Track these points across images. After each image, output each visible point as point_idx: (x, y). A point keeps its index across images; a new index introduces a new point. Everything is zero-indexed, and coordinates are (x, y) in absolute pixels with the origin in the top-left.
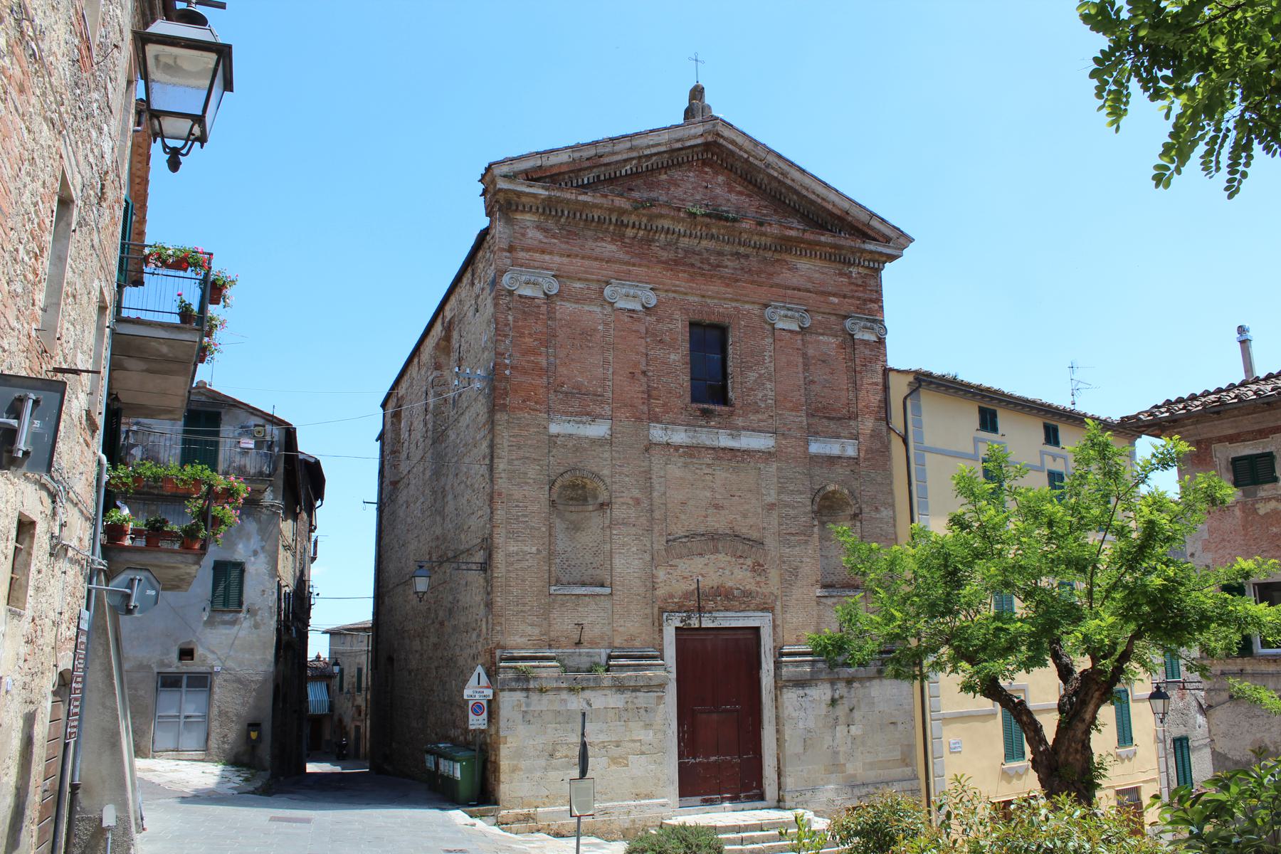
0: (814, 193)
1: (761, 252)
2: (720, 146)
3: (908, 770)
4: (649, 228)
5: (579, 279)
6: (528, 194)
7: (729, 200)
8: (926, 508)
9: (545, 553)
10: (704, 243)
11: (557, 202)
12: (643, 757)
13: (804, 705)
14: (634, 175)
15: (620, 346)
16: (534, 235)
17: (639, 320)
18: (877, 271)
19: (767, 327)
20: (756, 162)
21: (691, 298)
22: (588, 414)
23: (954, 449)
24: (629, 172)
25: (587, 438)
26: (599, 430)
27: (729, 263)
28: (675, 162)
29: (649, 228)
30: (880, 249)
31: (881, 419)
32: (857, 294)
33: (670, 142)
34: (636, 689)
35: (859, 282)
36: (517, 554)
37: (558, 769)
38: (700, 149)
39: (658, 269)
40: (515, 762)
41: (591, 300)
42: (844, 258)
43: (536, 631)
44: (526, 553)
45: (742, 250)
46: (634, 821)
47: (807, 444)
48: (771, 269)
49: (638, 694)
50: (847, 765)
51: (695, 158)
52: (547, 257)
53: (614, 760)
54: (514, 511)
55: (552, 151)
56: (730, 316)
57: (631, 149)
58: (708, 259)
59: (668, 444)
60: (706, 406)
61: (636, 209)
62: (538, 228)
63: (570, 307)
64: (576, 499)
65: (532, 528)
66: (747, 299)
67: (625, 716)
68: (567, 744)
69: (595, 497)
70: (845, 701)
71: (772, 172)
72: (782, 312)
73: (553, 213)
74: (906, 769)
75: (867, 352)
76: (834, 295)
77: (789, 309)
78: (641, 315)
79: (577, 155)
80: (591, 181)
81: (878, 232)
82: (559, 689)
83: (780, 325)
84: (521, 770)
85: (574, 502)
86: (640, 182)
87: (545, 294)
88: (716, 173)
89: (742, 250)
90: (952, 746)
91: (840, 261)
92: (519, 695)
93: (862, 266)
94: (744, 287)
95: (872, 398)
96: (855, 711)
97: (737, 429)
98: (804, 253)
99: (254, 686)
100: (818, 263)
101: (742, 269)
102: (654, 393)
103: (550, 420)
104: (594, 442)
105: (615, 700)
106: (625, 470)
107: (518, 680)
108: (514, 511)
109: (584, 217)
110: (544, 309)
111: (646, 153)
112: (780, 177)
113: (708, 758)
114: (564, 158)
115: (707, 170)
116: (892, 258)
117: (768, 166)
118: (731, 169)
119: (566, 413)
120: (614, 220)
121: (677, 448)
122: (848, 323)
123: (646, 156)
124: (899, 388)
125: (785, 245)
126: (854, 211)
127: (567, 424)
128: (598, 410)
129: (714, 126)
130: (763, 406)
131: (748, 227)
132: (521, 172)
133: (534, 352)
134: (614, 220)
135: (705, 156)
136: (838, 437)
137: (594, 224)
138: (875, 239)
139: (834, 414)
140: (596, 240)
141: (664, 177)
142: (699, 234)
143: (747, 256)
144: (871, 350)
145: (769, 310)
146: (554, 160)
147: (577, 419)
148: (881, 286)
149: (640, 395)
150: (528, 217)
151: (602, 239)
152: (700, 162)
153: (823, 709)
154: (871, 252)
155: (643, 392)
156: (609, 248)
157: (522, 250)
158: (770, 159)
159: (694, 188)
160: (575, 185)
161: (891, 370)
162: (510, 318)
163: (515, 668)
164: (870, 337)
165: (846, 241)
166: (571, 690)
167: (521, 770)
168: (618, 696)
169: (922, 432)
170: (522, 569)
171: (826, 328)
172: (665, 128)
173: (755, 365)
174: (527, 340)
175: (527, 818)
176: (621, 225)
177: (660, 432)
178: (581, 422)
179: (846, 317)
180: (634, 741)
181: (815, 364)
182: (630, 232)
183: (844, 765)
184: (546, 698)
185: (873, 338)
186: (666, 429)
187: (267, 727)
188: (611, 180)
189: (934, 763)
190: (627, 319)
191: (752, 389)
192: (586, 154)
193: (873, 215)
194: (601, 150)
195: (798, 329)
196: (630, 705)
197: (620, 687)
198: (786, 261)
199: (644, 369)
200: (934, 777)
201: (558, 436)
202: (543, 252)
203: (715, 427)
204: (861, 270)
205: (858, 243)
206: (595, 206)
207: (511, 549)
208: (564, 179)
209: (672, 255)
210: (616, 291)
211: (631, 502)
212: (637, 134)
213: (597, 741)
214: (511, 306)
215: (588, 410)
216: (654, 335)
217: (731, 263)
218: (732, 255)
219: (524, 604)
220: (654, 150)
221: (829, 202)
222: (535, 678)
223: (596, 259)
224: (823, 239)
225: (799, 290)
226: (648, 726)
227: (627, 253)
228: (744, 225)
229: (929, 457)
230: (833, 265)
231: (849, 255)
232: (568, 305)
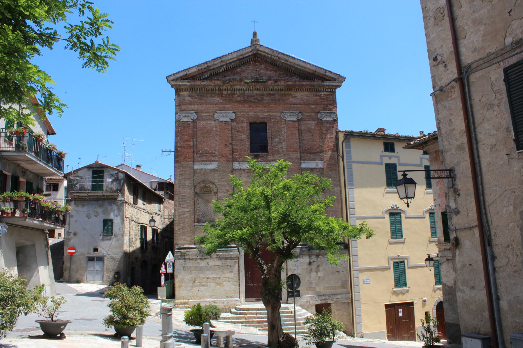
0: (300, 66)
1: (279, 92)
2: (260, 54)
3: (345, 290)
4: (231, 90)
5: (205, 112)
6: (183, 85)
7: (266, 74)
8: (352, 185)
9: (192, 211)
10: (255, 92)
11: (195, 86)
12: (229, 283)
13: (297, 264)
14: (225, 71)
15: (221, 135)
16: (188, 99)
17: (228, 124)
18: (334, 93)
19: (283, 120)
20: (275, 58)
21: (250, 114)
22: (209, 161)
23: (369, 160)
24: (223, 70)
25: (209, 169)
26: (213, 166)
27: (266, 98)
28: (242, 63)
29: (231, 90)
30: (331, 84)
31: (335, 151)
32: (324, 103)
33: (237, 56)
34: (226, 259)
35: (325, 98)
36: (182, 212)
37: (196, 287)
38: (252, 57)
39: (236, 104)
40: (181, 284)
41: (210, 119)
42: (316, 89)
43: (189, 239)
44: (185, 212)
45: (271, 92)
46: (225, 306)
47: (300, 164)
48: (284, 98)
49: (227, 260)
50: (316, 288)
51: (251, 60)
52: (193, 106)
53: (218, 284)
54: (181, 197)
55: (189, 68)
56: (267, 118)
57: (222, 62)
58: (257, 98)
59: (241, 169)
60: (256, 153)
61: (224, 84)
62: (189, 96)
63: (202, 123)
64: (208, 191)
65: (188, 203)
66: (274, 111)
67: (222, 268)
68: (200, 278)
69: (214, 190)
70: (315, 263)
71: (281, 60)
72: (288, 114)
73: (194, 90)
74: (343, 290)
75: (328, 125)
76: (313, 104)
77: (292, 113)
78: (230, 123)
79: (200, 68)
80: (208, 76)
81: (330, 77)
82: (196, 259)
83: (288, 119)
84: (183, 286)
85: (207, 193)
86: (229, 73)
87: (192, 120)
88: (261, 65)
89: (271, 92)
90: (365, 281)
91: (314, 91)
92: (182, 261)
93: (325, 91)
94: (272, 107)
95: (330, 143)
96: (320, 267)
97: (270, 161)
98: (298, 90)
99: (117, 260)
100: (305, 93)
101: (272, 100)
102: (235, 151)
103: (194, 164)
104: (211, 170)
105: (218, 263)
106: (223, 180)
107: (181, 256)
108: (181, 197)
109: (205, 89)
110: (192, 125)
111: (228, 62)
112: (285, 62)
113: (259, 284)
114: (195, 70)
115: (257, 64)
116: (339, 86)
117: (280, 58)
118: (266, 62)
119: (201, 161)
120: (217, 89)
121: (244, 170)
122: (319, 115)
123: (229, 63)
124: (341, 137)
125: (289, 88)
126: (318, 70)
127: (201, 165)
128: (213, 159)
129: (255, 47)
130: (281, 151)
131: (271, 83)
132: (179, 78)
133: (188, 140)
134: (217, 89)
135: (255, 59)
136: (315, 160)
137: (210, 92)
138: (329, 80)
139: (313, 151)
140: (211, 97)
141: (239, 70)
142: (252, 89)
143: (274, 95)
144: (330, 124)
145: (283, 114)
146: (191, 71)
147: (205, 163)
148: (336, 98)
149: (229, 152)
150: (185, 93)
151: (214, 97)
152: (254, 62)
153: (306, 266)
154: (328, 85)
155: (230, 151)
156: (217, 99)
157: (183, 105)
158: (280, 56)
159: (251, 72)
160: (202, 78)
161: (339, 131)
162: (179, 129)
163: (181, 252)
164: (329, 119)
165: (316, 83)
166: (201, 259)
167: (183, 286)
168: (219, 261)
169: (351, 156)
170: (184, 217)
171: (310, 118)
172: (234, 52)
173: (278, 136)
174: (185, 137)
175: (185, 303)
176: (220, 90)
177: (237, 165)
178: (206, 164)
179: (318, 113)
180: (225, 277)
181: (305, 133)
182: (225, 92)
183: (315, 288)
184: (191, 262)
185: (331, 119)
186: (240, 164)
187: (122, 273)
188: (217, 74)
189: (354, 288)
190: (223, 125)
191: (276, 145)
192: (203, 67)
193: (326, 71)
194: (209, 65)
195: (296, 120)
196: (224, 265)
197: (220, 258)
198: (291, 94)
199: (231, 142)
200: (354, 293)
201: (197, 170)
202: (191, 105)
203: (260, 161)
204: (325, 93)
205: (321, 83)
206: (208, 85)
207: (180, 210)
208: (197, 77)
209: (242, 99)
210: (219, 115)
211: (225, 191)
212: (223, 56)
213: (211, 277)
214: (180, 125)
215: (209, 159)
216: (235, 129)
217: (267, 98)
218: (267, 95)
219: (185, 229)
220: (231, 61)
221: (307, 68)
222: (187, 255)
223: (211, 104)
224: (304, 83)
225: (296, 105)
226: (231, 272)
227: (224, 100)
228: (269, 83)
229: (354, 165)
230: (312, 93)
231: (318, 88)
232: (201, 122)
